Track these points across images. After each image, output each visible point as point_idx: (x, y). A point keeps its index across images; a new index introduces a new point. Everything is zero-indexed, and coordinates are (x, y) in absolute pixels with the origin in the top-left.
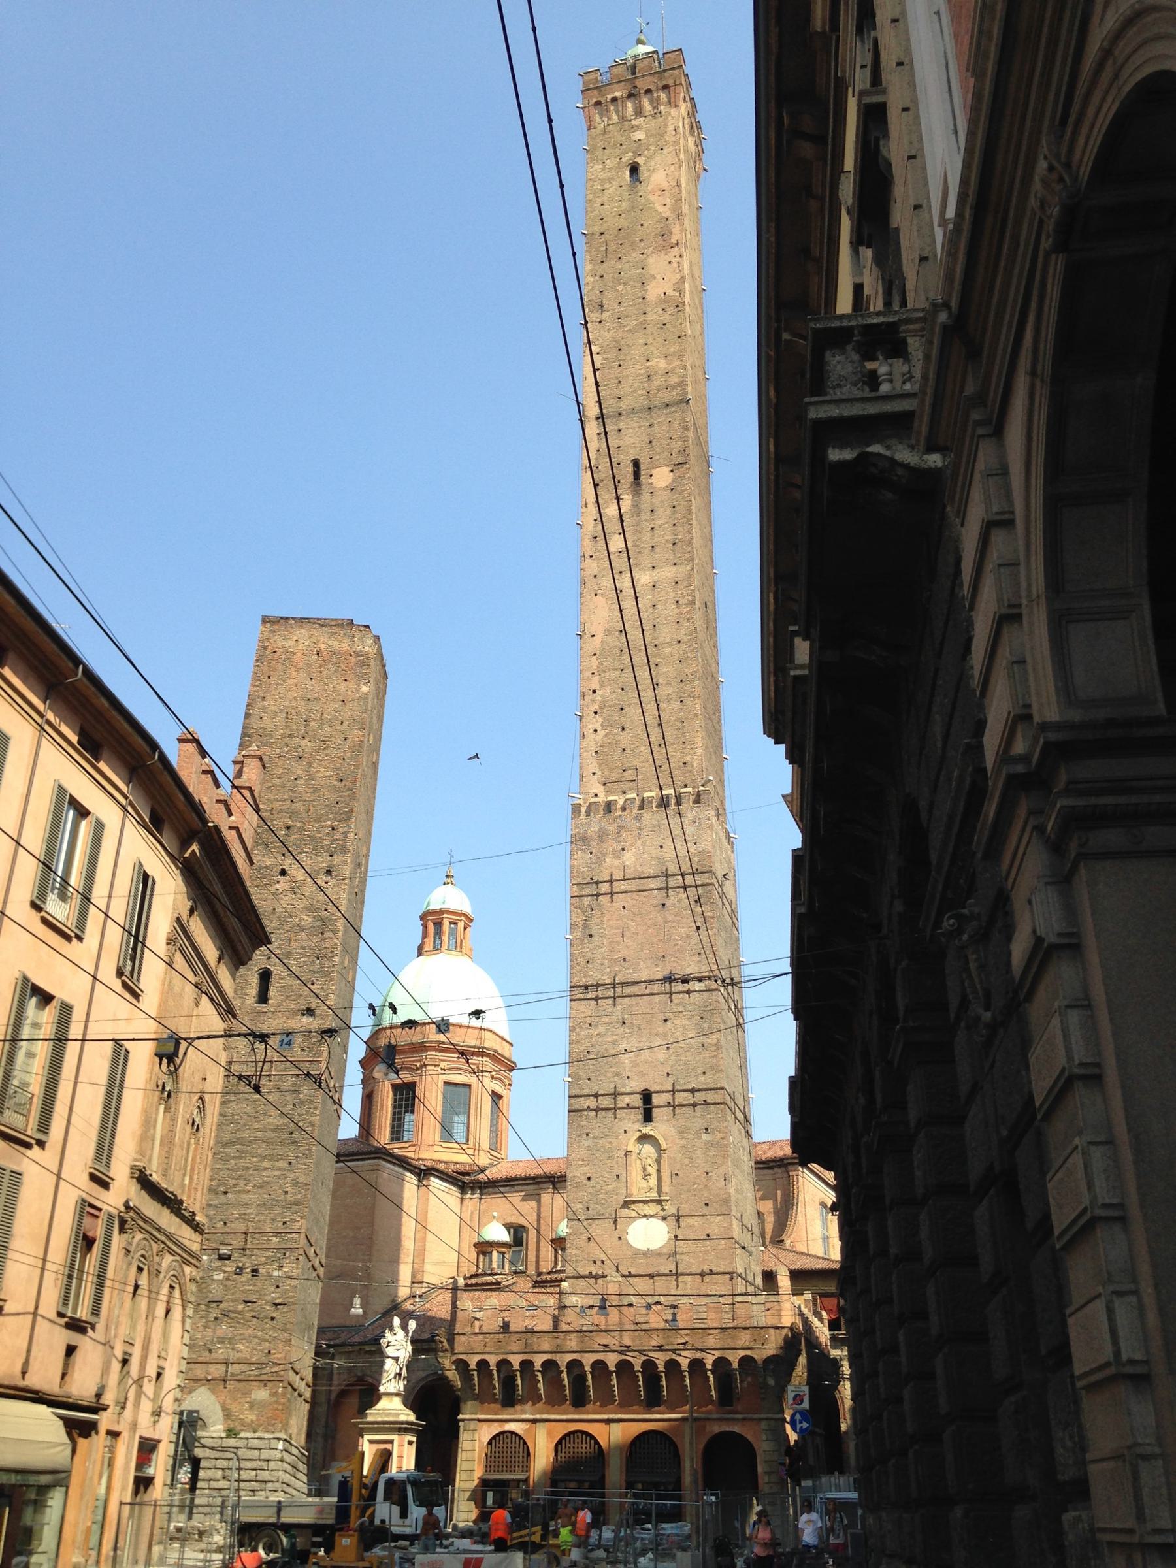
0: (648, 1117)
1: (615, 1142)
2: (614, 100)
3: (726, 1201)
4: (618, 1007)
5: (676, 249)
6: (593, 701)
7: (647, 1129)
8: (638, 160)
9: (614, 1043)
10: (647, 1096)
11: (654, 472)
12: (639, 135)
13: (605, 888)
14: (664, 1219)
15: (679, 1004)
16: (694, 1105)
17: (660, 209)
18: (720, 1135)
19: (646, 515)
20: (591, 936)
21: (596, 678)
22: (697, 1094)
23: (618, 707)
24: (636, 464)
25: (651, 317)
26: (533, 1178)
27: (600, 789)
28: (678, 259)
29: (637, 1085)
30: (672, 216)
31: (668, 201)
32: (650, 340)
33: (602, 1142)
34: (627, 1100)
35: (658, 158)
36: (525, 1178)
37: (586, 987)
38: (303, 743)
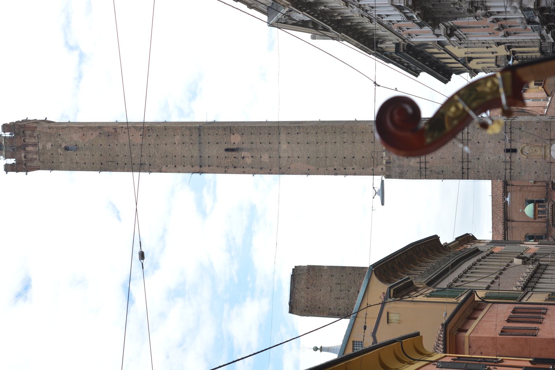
0: (515, 151)
1: (523, 163)
2: (25, 157)
3: (546, 122)
4: (472, 160)
5: (117, 130)
6: (339, 169)
7: (519, 151)
8: (63, 146)
9: (486, 162)
10: (508, 151)
11: (233, 142)
12: (49, 146)
13: (423, 165)
14: (551, 145)
15: (472, 137)
16: (511, 132)
17: (94, 136)
18: (523, 124)
19: (254, 146)
20: (442, 171)
21: (329, 168)
22: (507, 131)
23: (343, 159)
24: (227, 150)
25: (152, 142)
26: (505, 230)
27: (380, 168)
28: (123, 129)
29: (502, 155)
30: (99, 131)
31: (90, 133)
32: (165, 142)
33: (523, 168)
34: (508, 158)
35: (64, 137)
36: (505, 234)
37: (463, 173)
38: (352, 291)
